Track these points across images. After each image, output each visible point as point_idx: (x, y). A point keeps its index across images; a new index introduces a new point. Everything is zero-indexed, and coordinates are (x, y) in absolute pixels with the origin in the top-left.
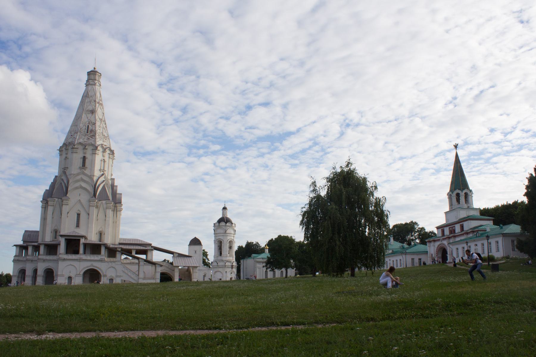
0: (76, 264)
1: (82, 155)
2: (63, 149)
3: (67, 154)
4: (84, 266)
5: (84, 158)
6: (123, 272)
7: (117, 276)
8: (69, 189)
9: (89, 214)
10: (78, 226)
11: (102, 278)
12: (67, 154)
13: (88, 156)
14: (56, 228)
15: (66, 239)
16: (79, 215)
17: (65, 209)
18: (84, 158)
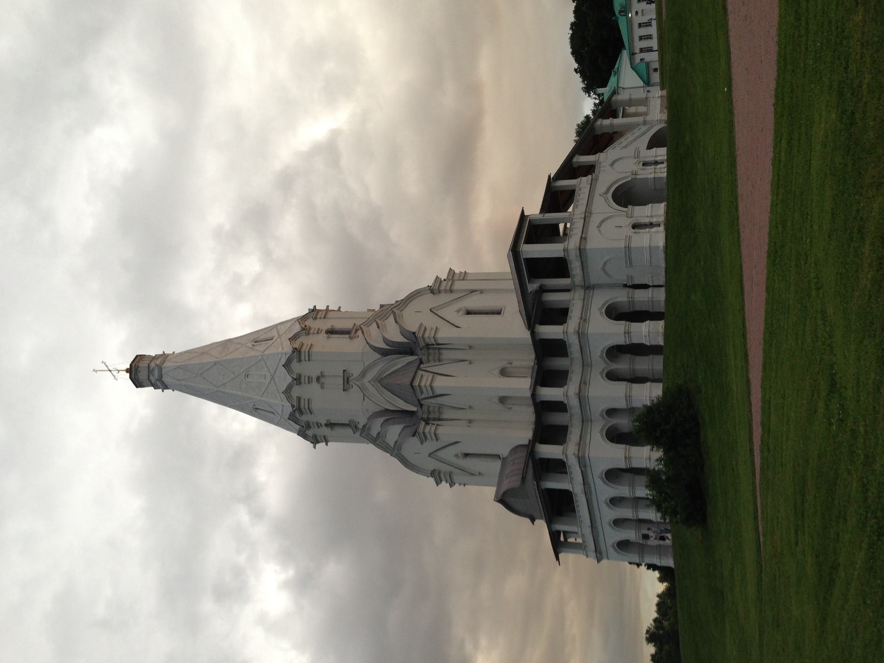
0: (595, 220)
1: (323, 335)
2: (296, 391)
3: (310, 380)
4: (604, 206)
5: (331, 332)
6: (625, 147)
7: (637, 155)
8: (400, 339)
9: (473, 291)
10: (498, 313)
11: (638, 177)
12: (310, 380)
13: (326, 325)
14: (497, 372)
15: (527, 242)
16: (469, 313)
17: (445, 333)
18: (331, 332)
